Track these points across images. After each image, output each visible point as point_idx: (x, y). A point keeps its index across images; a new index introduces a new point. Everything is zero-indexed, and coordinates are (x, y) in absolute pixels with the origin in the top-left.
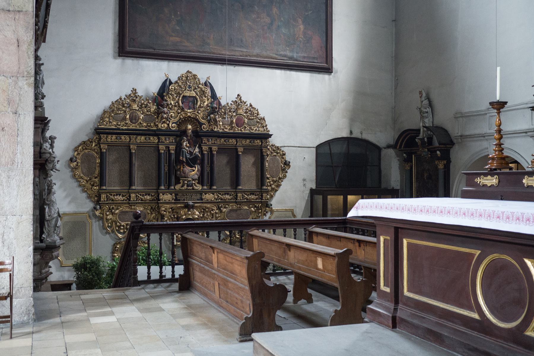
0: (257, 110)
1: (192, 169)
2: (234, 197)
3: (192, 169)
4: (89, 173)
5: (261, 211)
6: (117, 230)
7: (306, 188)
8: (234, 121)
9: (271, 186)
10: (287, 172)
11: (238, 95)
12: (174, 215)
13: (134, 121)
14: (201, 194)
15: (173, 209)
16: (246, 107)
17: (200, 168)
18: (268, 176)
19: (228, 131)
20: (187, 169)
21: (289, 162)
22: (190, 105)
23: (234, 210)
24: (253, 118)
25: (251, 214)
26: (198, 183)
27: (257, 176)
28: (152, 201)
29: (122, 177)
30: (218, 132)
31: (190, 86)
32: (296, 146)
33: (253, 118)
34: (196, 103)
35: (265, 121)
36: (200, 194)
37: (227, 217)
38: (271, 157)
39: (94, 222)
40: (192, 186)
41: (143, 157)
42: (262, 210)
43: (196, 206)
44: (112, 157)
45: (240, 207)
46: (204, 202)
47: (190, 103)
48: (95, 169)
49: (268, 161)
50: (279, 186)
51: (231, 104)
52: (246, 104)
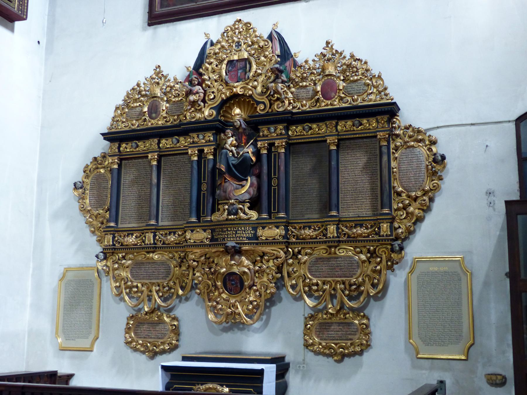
0: (366, 63)
1: (240, 183)
2: (322, 232)
3: (240, 183)
4: (99, 203)
5: (379, 259)
6: (127, 293)
7: (494, 210)
8: (319, 88)
9: (405, 208)
10: (440, 179)
11: (328, 43)
12: (210, 268)
13: (154, 115)
14: (255, 229)
15: (207, 256)
16: (344, 61)
17: (255, 182)
18: (400, 189)
19: (308, 110)
20: (230, 185)
21: (443, 158)
22: (239, 74)
23: (323, 258)
24: (356, 78)
25: (358, 266)
26: (250, 208)
27: (373, 189)
28: (179, 243)
29: (142, 208)
30: (285, 112)
31: (240, 43)
32: (464, 123)
33: (356, 78)
34: (248, 69)
35: (382, 80)
36: (252, 228)
37: (310, 272)
38: (404, 151)
39: (105, 281)
40: (236, 213)
41: (172, 173)
42: (381, 258)
43: (246, 251)
44: (129, 177)
45: (335, 253)
46: (260, 243)
47: (240, 71)
48: (107, 197)
49: (396, 158)
50: (427, 209)
51: (314, 61)
52: (342, 56)
